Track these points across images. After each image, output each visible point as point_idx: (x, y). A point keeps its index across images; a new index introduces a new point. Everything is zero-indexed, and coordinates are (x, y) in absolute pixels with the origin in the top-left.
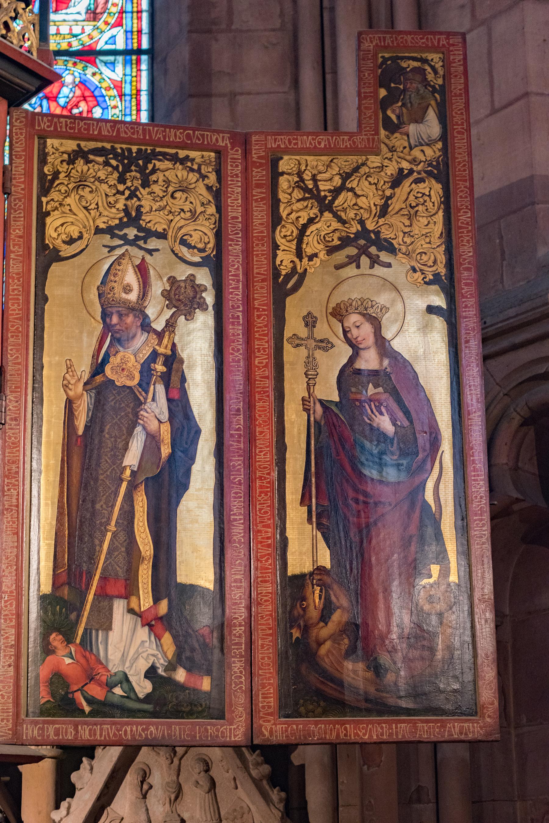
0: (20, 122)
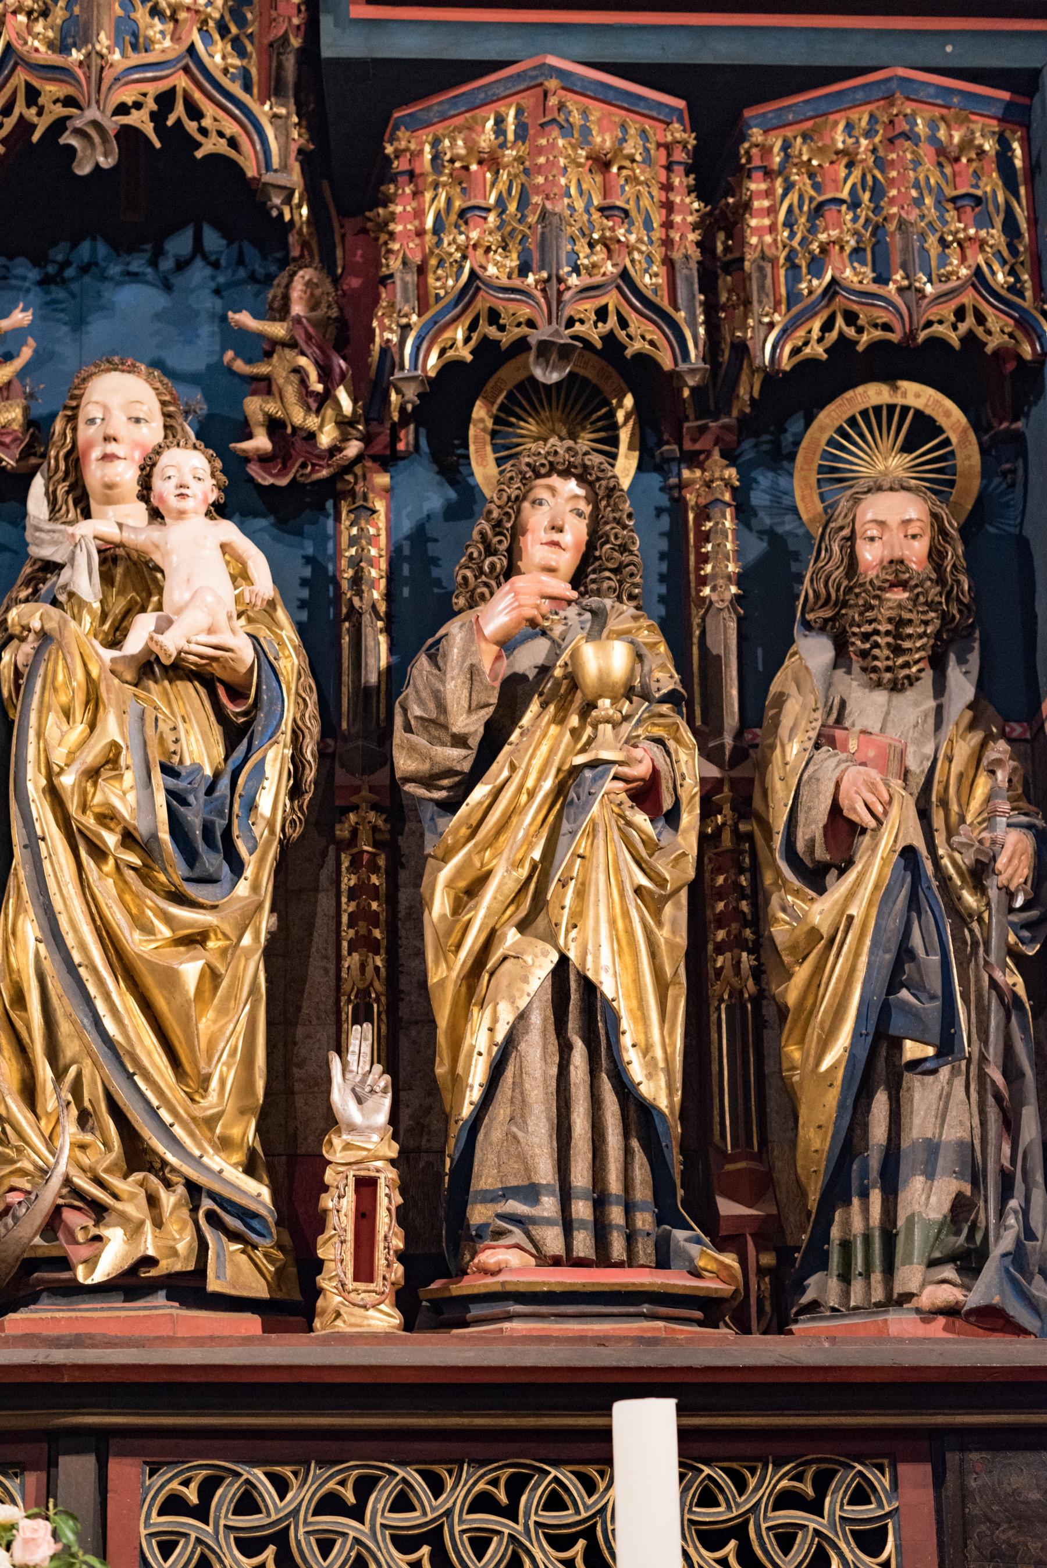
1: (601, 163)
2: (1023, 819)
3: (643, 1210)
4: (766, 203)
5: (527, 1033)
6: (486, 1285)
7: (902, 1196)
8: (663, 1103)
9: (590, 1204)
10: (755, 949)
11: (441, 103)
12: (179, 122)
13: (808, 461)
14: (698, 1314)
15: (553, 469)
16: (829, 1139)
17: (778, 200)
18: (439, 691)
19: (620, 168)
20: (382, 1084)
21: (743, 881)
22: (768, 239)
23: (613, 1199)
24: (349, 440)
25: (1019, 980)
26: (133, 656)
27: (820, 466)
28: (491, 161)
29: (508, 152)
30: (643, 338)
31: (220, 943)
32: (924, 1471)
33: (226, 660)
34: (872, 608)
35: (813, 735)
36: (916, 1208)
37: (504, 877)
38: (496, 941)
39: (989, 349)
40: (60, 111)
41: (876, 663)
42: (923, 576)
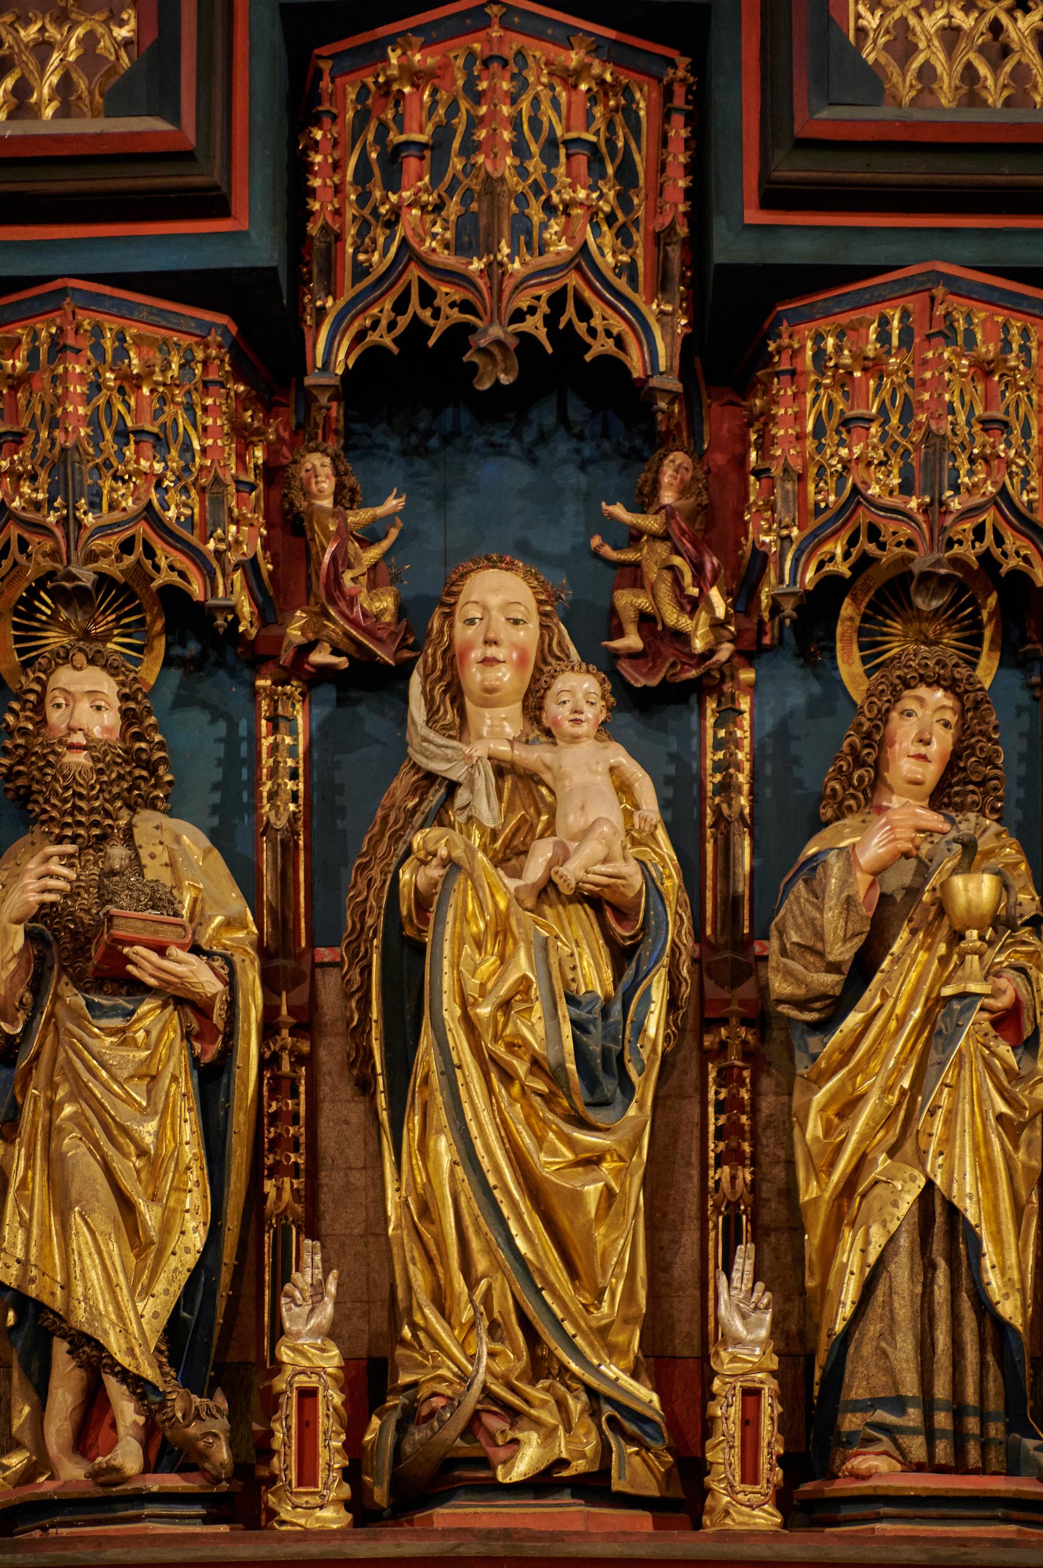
5: (896, 1255)
6: (859, 1489)
8: (1018, 1322)
9: (950, 1415)
12: (570, 322)
18: (814, 919)
20: (765, 1301)
23: (970, 1410)
26: (533, 885)
28: (875, 367)
30: (1017, 553)
31: (614, 1164)
38: (867, 1164)
40: (456, 315)
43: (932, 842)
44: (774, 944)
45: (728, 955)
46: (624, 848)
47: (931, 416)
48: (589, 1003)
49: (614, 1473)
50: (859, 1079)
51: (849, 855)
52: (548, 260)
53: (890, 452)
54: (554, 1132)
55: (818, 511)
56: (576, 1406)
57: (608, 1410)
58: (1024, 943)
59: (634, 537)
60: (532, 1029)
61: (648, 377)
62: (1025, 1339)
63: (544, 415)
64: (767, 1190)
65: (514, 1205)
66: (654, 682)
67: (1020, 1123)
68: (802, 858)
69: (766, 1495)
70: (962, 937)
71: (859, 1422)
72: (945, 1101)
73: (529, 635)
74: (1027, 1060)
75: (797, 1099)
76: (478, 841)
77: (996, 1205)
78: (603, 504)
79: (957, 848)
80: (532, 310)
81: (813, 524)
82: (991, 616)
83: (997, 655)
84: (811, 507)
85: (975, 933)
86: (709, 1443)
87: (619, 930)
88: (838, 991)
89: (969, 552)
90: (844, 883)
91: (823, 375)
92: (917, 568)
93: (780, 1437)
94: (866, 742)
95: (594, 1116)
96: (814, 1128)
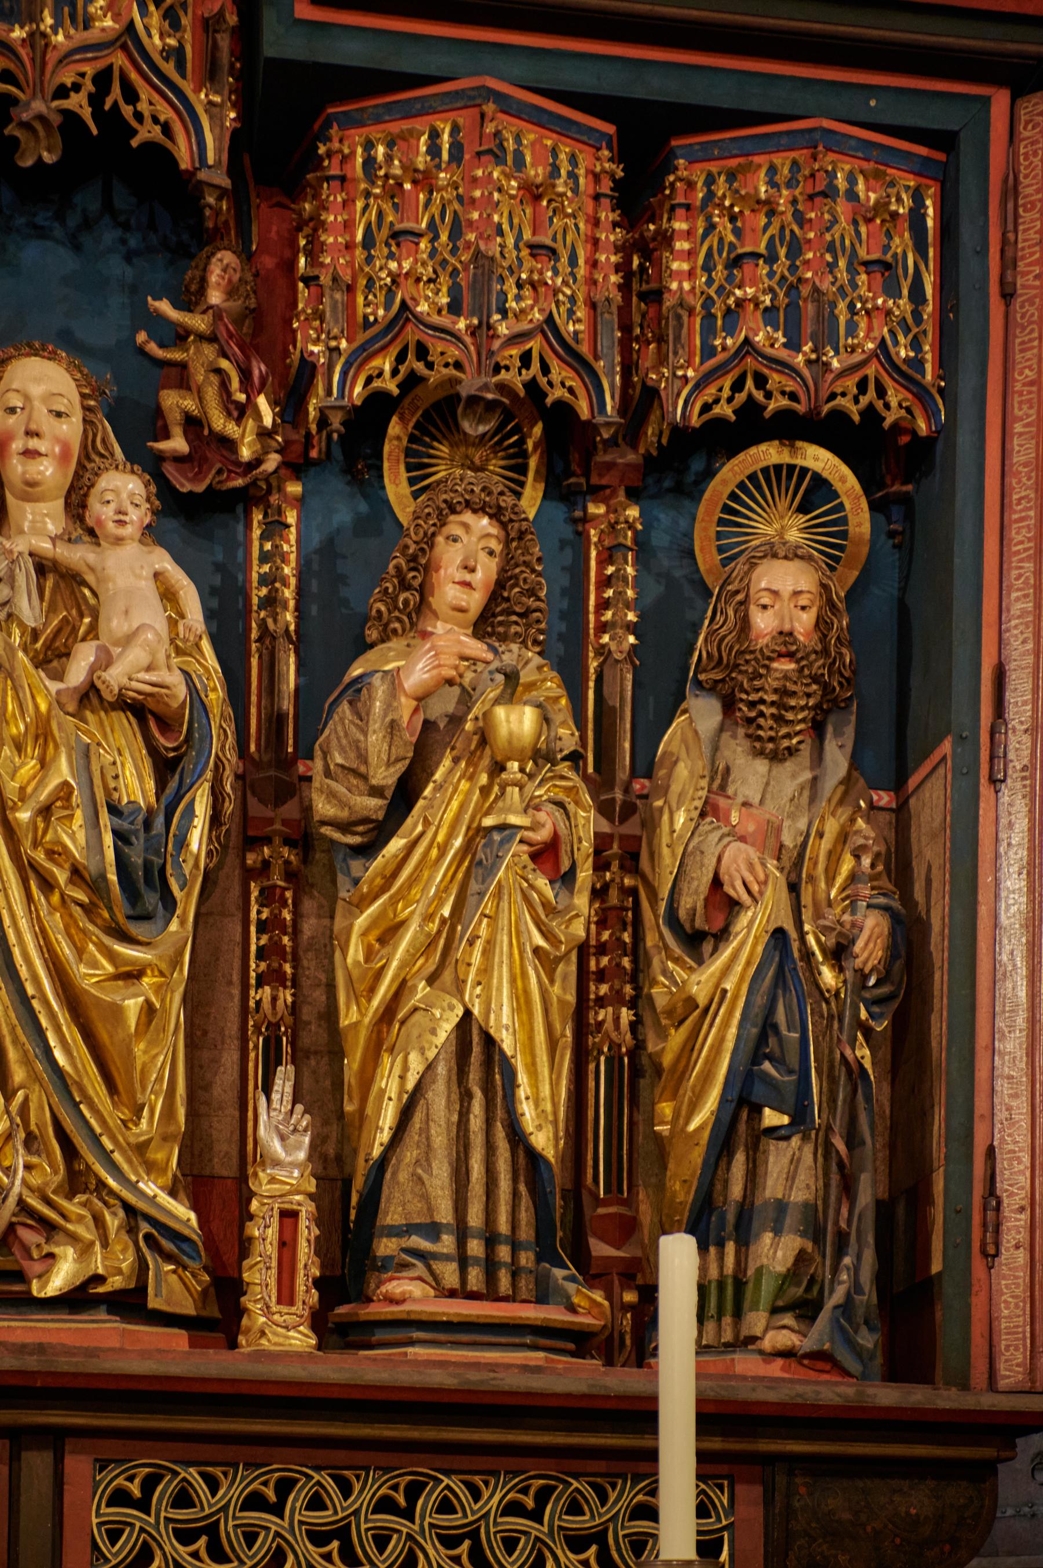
0: (1033, 128)
1: (533, 193)
2: (882, 900)
3: (526, 1249)
4: (686, 246)
5: (434, 1082)
6: (393, 1313)
7: (752, 1248)
8: (550, 1154)
9: (483, 1243)
10: (633, 1004)
11: (376, 106)
12: (115, 103)
13: (709, 513)
14: (571, 1346)
15: (468, 504)
16: (692, 1193)
17: (699, 240)
18: (359, 741)
19: (550, 201)
20: (304, 1123)
21: (626, 937)
22: (686, 286)
23: (502, 1239)
24: (267, 453)
25: (867, 1052)
26: (75, 688)
27: (720, 519)
29: (442, 175)
31: (155, 980)
32: (757, 1490)
33: (161, 696)
34: (761, 676)
35: (699, 804)
36: (765, 1261)
37: (416, 932)
38: (406, 991)
39: (887, 424)
41: (761, 733)
42: (808, 650)
43: (475, 671)
44: (318, 764)
45: (272, 773)
46: (168, 657)
47: (480, 236)
48: (131, 814)
49: (151, 1291)
50: (400, 905)
51: (394, 678)
52: (93, 35)
53: (439, 270)
54: (94, 943)
55: (367, 324)
56: (113, 1222)
57: (145, 1228)
58: (563, 778)
59: (180, 336)
60: (73, 836)
61: (196, 169)
62: (556, 1170)
63: (88, 200)
64: (307, 1013)
65: (52, 1016)
66: (200, 488)
67: (556, 957)
68: (347, 679)
69: (301, 1316)
70: (503, 769)
71: (394, 1246)
72: (483, 931)
73: (72, 429)
74: (564, 894)
75: (339, 923)
76: (18, 640)
77: (531, 1038)
78: (149, 298)
79: (500, 678)
80: (77, 87)
81: (361, 337)
82: (536, 446)
83: (541, 486)
84: (360, 319)
85: (516, 765)
86: (246, 1263)
87: (162, 740)
88: (380, 815)
89: (515, 379)
90: (388, 707)
91: (373, 183)
92: (464, 391)
93: (316, 1259)
94: (412, 565)
95: (135, 929)
96: (355, 952)
